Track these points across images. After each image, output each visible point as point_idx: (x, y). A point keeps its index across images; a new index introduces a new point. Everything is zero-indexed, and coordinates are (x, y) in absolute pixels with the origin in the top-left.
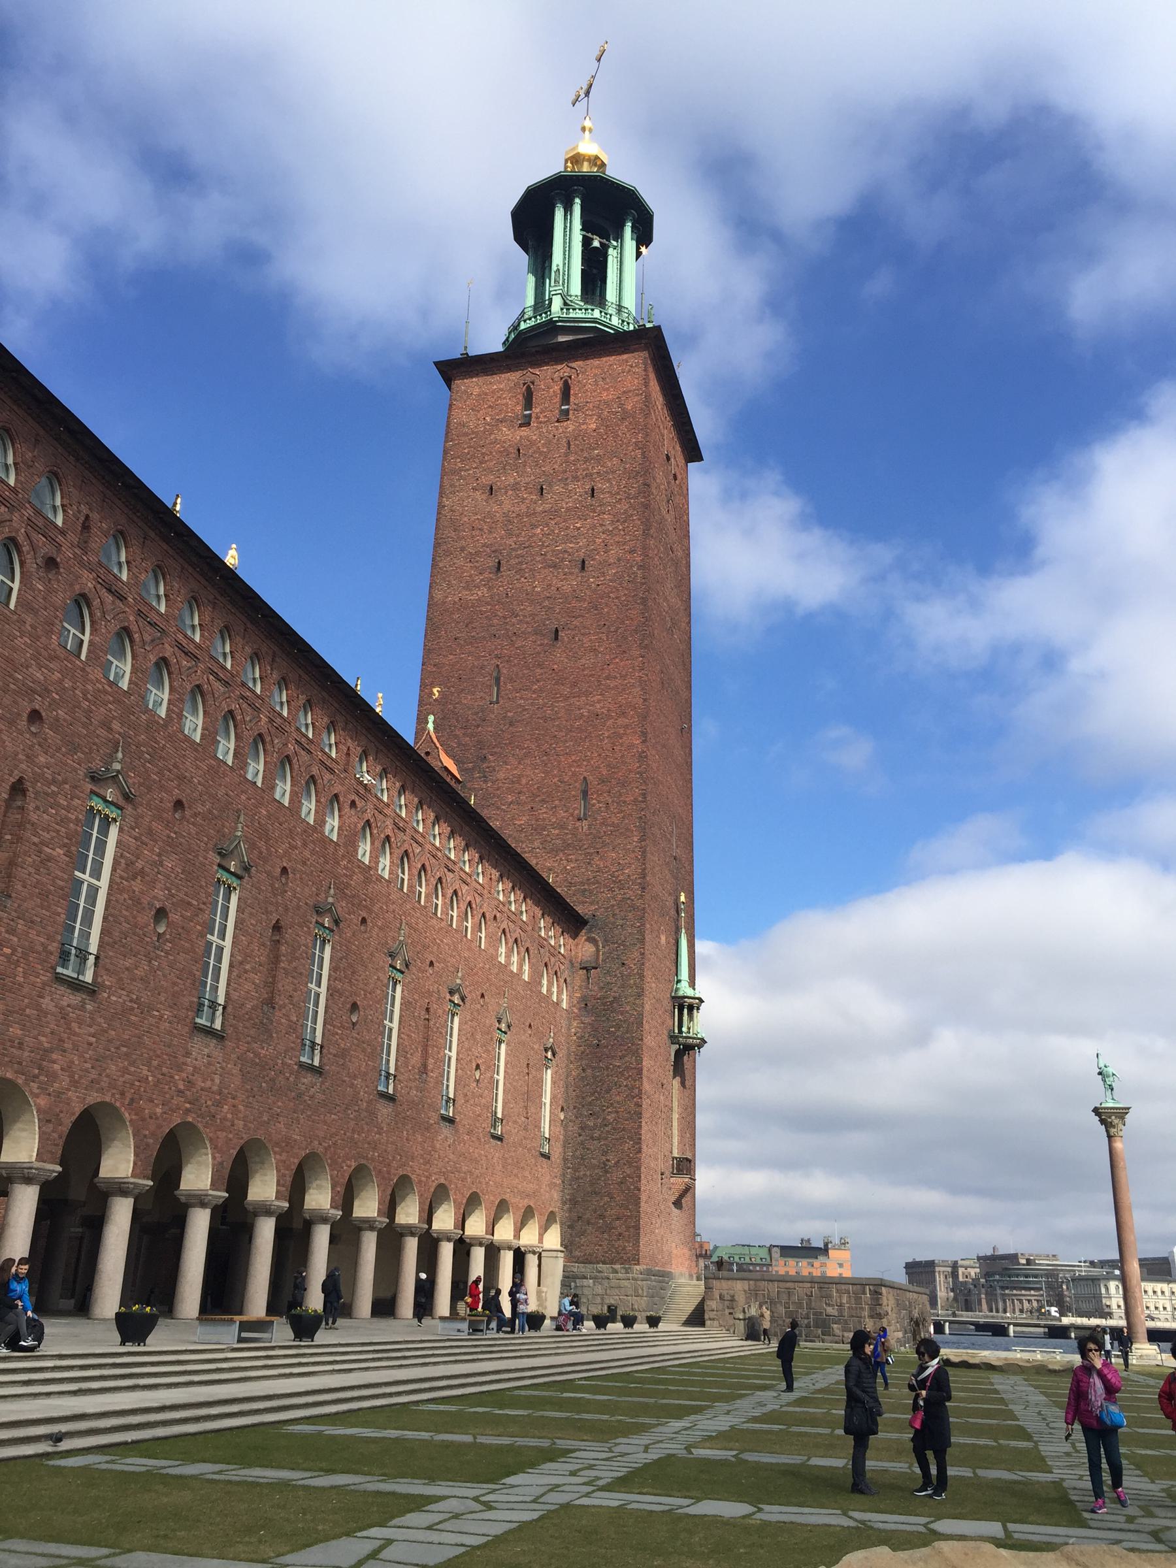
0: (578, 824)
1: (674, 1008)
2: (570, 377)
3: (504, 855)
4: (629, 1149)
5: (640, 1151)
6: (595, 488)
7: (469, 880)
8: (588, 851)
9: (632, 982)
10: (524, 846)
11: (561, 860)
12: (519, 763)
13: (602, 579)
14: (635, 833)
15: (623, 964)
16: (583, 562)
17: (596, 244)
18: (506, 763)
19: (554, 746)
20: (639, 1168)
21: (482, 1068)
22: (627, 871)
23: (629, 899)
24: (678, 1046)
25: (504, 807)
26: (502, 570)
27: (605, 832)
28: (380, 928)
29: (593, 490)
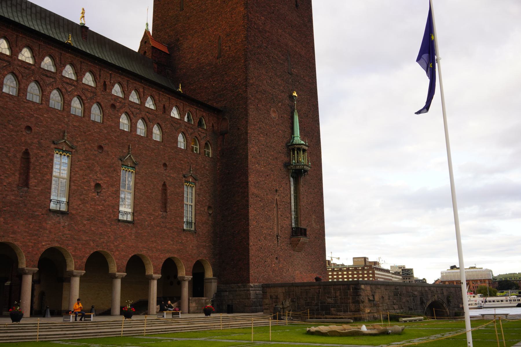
0: (218, 61)
1: (291, 151)
5: (248, 225)
7: (75, 83)
8: (222, 74)
9: (242, 137)
10: (195, 79)
11: (211, 81)
12: (192, 38)
14: (242, 58)
15: (239, 129)
18: (187, 39)
19: (206, 24)
20: (248, 234)
21: (104, 186)
22: (239, 80)
23: (240, 94)
24: (292, 170)
25: (186, 62)
27: (229, 62)
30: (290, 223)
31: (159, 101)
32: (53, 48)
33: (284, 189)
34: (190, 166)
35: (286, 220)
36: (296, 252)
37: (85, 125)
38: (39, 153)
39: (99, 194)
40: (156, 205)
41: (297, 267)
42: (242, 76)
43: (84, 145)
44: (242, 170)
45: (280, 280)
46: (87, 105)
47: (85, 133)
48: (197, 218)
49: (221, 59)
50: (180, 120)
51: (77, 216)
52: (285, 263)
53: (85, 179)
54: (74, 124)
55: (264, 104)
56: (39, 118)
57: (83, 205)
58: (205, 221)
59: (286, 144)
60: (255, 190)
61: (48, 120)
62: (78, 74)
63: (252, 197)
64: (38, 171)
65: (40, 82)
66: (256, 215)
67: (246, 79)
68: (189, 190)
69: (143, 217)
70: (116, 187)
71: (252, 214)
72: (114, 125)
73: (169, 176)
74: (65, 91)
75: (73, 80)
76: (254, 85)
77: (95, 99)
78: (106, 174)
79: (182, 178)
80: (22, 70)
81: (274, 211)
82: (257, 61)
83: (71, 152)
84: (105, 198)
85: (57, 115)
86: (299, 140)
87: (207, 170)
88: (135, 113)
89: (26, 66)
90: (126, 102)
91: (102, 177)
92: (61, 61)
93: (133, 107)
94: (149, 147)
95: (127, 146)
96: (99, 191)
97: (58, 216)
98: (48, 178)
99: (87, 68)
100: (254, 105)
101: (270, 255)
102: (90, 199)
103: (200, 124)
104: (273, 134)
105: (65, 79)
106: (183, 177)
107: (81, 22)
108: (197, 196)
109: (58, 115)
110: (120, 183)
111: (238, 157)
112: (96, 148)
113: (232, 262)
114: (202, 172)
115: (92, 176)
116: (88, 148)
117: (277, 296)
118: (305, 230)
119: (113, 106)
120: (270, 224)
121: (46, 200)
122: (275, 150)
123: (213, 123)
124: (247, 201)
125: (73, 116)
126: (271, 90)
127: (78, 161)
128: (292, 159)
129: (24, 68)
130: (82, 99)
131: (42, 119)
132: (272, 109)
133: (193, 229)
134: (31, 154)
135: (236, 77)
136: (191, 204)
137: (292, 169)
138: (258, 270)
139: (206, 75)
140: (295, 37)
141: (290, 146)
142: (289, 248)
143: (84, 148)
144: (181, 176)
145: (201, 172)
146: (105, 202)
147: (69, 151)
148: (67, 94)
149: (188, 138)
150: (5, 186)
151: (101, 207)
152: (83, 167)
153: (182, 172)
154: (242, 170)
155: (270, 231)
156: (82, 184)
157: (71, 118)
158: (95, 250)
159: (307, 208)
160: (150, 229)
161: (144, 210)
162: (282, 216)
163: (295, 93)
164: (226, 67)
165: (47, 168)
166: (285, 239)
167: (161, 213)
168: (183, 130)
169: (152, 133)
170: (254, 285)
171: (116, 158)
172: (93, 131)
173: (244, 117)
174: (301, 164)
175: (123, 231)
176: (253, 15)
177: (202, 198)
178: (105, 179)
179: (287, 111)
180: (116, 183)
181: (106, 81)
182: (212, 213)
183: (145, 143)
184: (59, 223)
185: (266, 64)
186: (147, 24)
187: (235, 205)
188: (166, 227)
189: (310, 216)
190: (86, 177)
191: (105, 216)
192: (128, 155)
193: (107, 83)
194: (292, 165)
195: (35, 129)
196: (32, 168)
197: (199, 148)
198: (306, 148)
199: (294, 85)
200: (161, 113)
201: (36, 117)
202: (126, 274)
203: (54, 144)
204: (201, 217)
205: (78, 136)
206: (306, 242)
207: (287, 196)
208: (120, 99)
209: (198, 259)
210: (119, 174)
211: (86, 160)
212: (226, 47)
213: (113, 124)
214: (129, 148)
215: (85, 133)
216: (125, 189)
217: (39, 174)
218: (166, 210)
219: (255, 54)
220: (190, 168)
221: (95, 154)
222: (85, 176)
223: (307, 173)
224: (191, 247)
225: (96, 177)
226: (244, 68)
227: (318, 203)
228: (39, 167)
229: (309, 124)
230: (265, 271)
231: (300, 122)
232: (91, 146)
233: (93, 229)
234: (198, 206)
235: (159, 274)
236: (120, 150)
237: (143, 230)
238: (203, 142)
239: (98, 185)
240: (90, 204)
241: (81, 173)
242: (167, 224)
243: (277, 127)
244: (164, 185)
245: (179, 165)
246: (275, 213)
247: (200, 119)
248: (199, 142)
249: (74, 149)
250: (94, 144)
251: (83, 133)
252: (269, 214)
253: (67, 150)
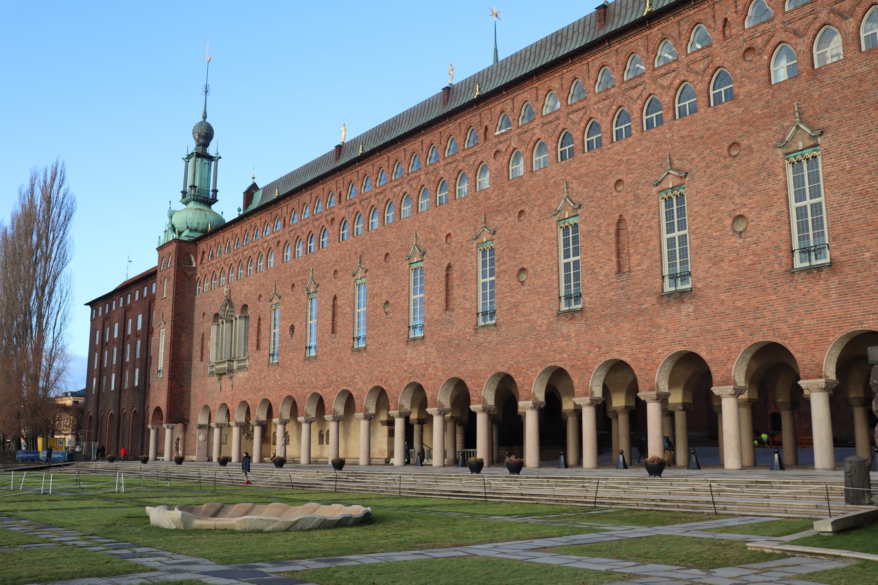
21: (751, 216)
28: (540, 205)
39: (743, 235)
54: (682, 135)
57: (715, 266)
64: (639, 240)
69: (856, 245)
84: (755, 238)
91: (744, 200)
93: (795, 20)
115: (724, 208)
150: (601, 280)
151: (751, 257)
190: (714, 215)
191: (761, 273)
217: (641, 244)
233: (739, 304)
241: (705, 211)
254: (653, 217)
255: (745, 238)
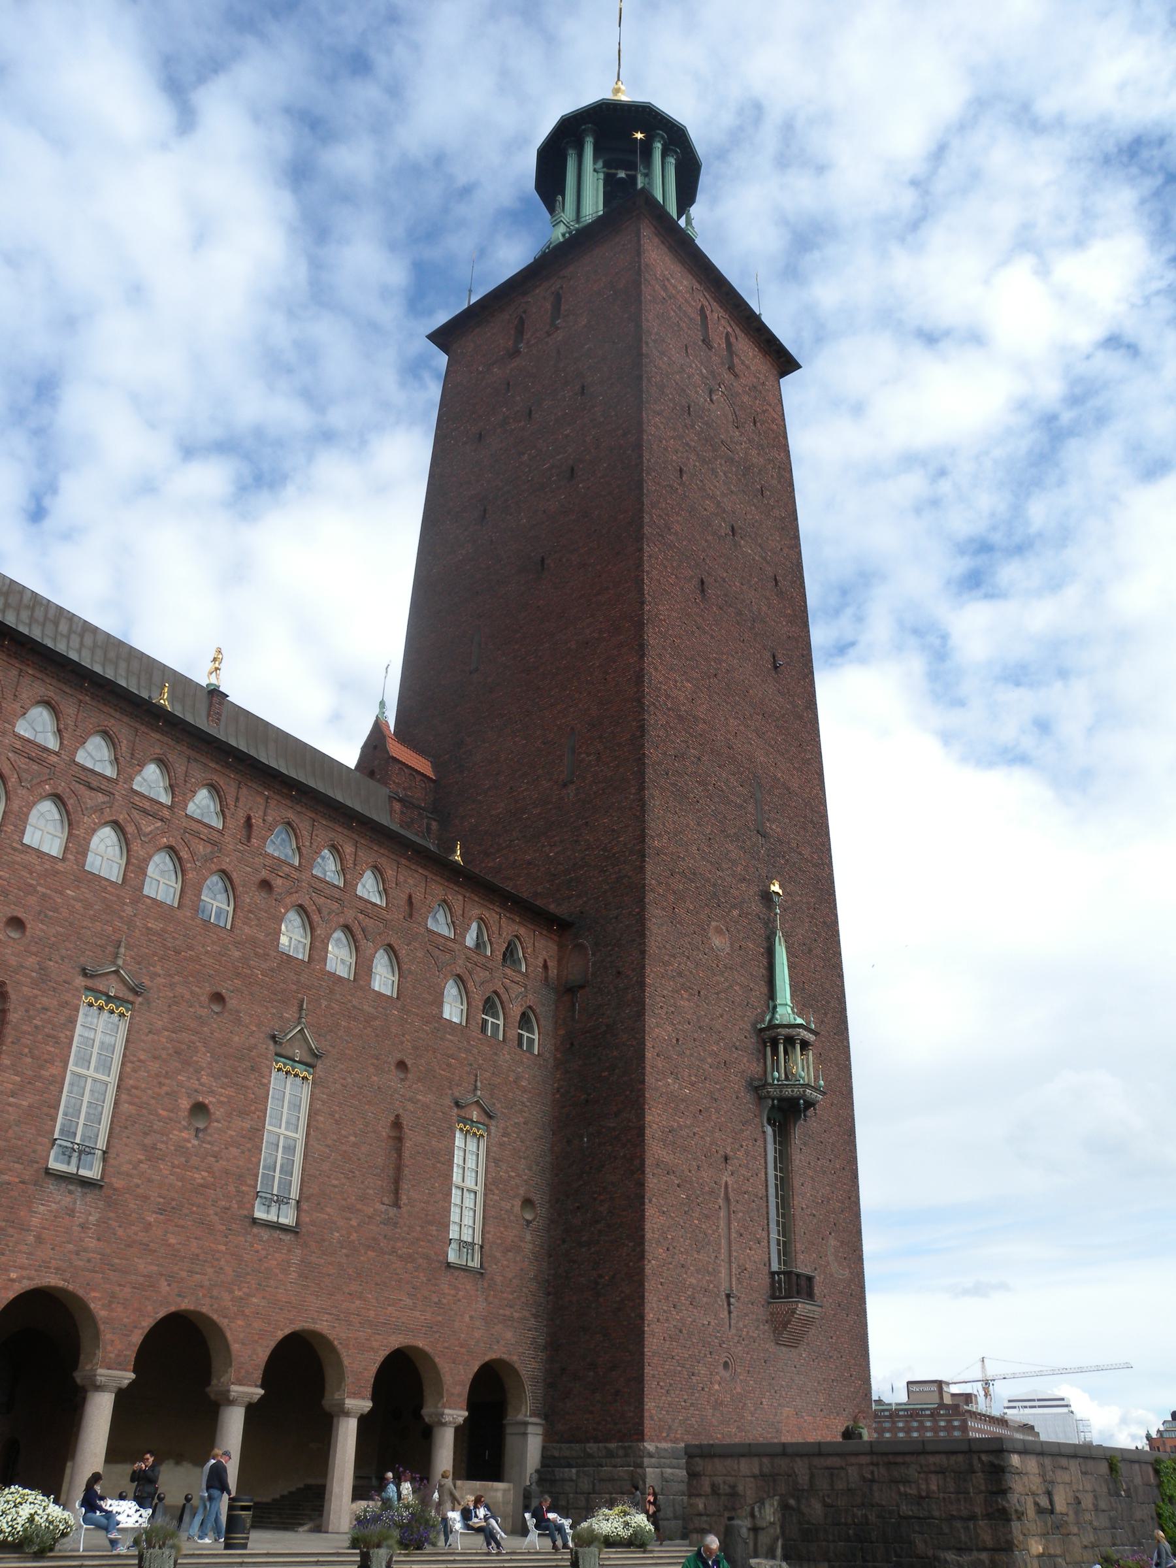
1: (765, 1046)
2: (561, 288)
3: (284, 791)
4: (628, 1255)
5: (641, 1256)
6: (586, 384)
7: (166, 813)
9: (630, 996)
11: (543, 846)
13: (592, 479)
15: (619, 973)
16: (572, 469)
17: (622, 174)
20: (641, 1284)
21: (218, 1112)
26: (487, 516)
27: (595, 793)
29: (583, 387)
30: (767, 1259)
31: (397, 884)
32: (117, 715)
33: (747, 1153)
34: (476, 1076)
35: (754, 1247)
36: (784, 1348)
37: (180, 930)
38: (36, 997)
39: (200, 1135)
40: (369, 1183)
41: (786, 1394)
42: (630, 828)
43: (172, 986)
44: (628, 1093)
45: (736, 1434)
46: (191, 875)
47: (178, 952)
48: (489, 1232)
49: (572, 787)
50: (454, 940)
51: (127, 1196)
52: (751, 1382)
53: (164, 1085)
54: (150, 925)
55: (691, 907)
56: (50, 898)
57: (149, 1163)
58: (512, 1242)
59: (754, 1025)
60: (665, 1153)
61: (77, 907)
62: (176, 789)
63: (655, 1172)
64: (26, 1050)
65: (66, 799)
66: (665, 1229)
67: (642, 838)
68: (472, 1145)
69: (327, 1217)
70: (252, 1120)
71: (654, 1226)
72: (262, 938)
73: (410, 1100)
74: (136, 831)
75: (161, 804)
76: (665, 854)
77: (215, 860)
78: (226, 1077)
79: (450, 1108)
80: (22, 763)
81: (718, 1218)
82: (672, 792)
83: (132, 1003)
84: (216, 1149)
85: (104, 894)
86: (789, 1014)
87: (524, 1090)
88: (325, 912)
89: (34, 755)
90: (304, 877)
91: (214, 1084)
92: (133, 750)
94: (358, 1009)
95: (296, 1002)
96: (201, 1126)
97: (70, 1192)
98: (55, 1072)
99: (203, 775)
100: (663, 909)
101: (705, 1356)
102: (173, 1148)
103: (509, 954)
104: (717, 994)
105: (138, 799)
106: (452, 1105)
107: (208, 682)
108: (493, 1164)
109: (107, 896)
110: (266, 1109)
111: (615, 1053)
112: (204, 999)
113: (591, 1374)
114: (510, 1094)
115: (184, 1079)
116: (182, 997)
117: (733, 1487)
118: (810, 1279)
119: (266, 885)
120: (708, 1257)
121: (40, 1139)
122: (723, 1039)
123: (547, 958)
124: (641, 1185)
125: (148, 901)
126: (710, 872)
127: (150, 1032)
128: (769, 1069)
129: (29, 758)
130: (180, 859)
131: (59, 900)
132: (713, 924)
133: (476, 1264)
134: (13, 996)
135: (613, 830)
136: (472, 1186)
137: (769, 1097)
138: (669, 1399)
139: (532, 830)
140: (773, 743)
141: (762, 1030)
142: (763, 1334)
143: (172, 995)
144: (448, 1101)
145: (505, 1096)
146: (217, 1161)
147: (128, 1002)
148: (139, 841)
149: (473, 992)
151: (205, 1174)
152: (163, 1049)
153: (450, 1089)
154: (628, 1093)
155: (708, 1278)
156: (153, 1101)
157: (144, 907)
158: (173, 1309)
159: (814, 1215)
160: (347, 1256)
161: (332, 1196)
162: (741, 1235)
163: (777, 886)
164: (587, 806)
165: (56, 1043)
166: (750, 1305)
167: (383, 1210)
168: (459, 971)
169: (369, 972)
170: (657, 1447)
171: (261, 1035)
172: (201, 949)
173: (634, 940)
174: (797, 1082)
175: (264, 1253)
176: (664, 675)
177: (507, 1172)
178: (223, 1091)
179: (755, 933)
180: (253, 1108)
181: (252, 815)
182: (534, 1220)
183: (349, 998)
184: (71, 1212)
185: (698, 802)
186: (382, 704)
187: (602, 1197)
188: (394, 1251)
189: (823, 1239)
190: (167, 1081)
191: (213, 1205)
192: (296, 1027)
193: (254, 821)
194: (772, 1085)
195: (35, 928)
196: (10, 1040)
197: (504, 1024)
198: (811, 1037)
199: (774, 866)
200: (401, 917)
201: (44, 895)
202: (262, 1392)
203: (85, 975)
204: (502, 1229)
205: (156, 958)
206: (813, 1318)
207: (757, 1175)
208: (286, 869)
209: (487, 1359)
210: (266, 1081)
211: (173, 1032)
212: (589, 755)
213: (261, 936)
214: (301, 1008)
215: (178, 952)
216: (280, 1128)
217: (29, 1060)
218: (397, 1201)
219: (667, 774)
220: (476, 1081)
221: (201, 1017)
222: (166, 1078)
223: (815, 1109)
224: (467, 1318)
225: (195, 1084)
226: (639, 808)
227: (843, 1203)
228: (31, 1038)
229: (814, 973)
230: (692, 1405)
231: (791, 967)
232: (192, 992)
233: (172, 1241)
234: (493, 1194)
235: (363, 1398)
236: (275, 1011)
237: (324, 1257)
238: (516, 1011)
239: (199, 1109)
240: (169, 1164)
241: (155, 1066)
242: (399, 1244)
243: (726, 974)
244: (397, 1125)
245: (443, 1070)
246: (722, 1223)
247: (509, 945)
248: (503, 1008)
249: (139, 996)
250: (200, 988)
251: (173, 953)
252: (703, 1226)
253: (121, 995)
254: (64, 1024)
255: (203, 1142)
